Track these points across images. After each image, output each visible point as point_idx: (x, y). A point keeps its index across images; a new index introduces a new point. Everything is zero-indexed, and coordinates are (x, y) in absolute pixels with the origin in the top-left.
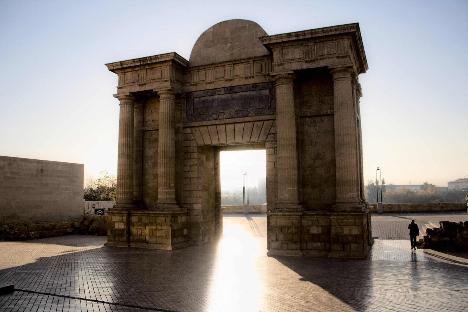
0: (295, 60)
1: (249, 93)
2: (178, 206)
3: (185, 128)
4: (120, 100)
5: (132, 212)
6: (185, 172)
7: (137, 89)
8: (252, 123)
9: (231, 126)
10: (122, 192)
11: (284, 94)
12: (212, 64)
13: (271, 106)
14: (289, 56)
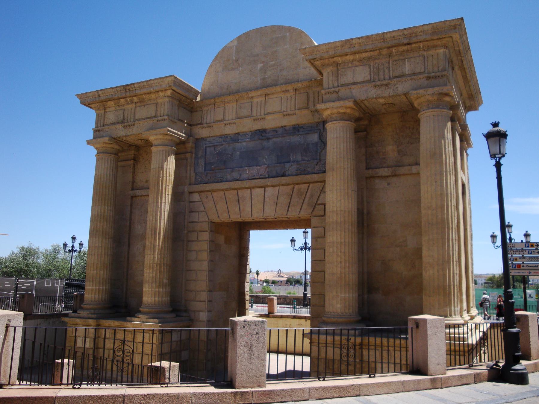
2: (173, 315)
3: (191, 193)
4: (96, 148)
6: (188, 261)
7: (120, 131)
8: (290, 187)
9: (260, 191)
10: (92, 290)
13: (320, 160)
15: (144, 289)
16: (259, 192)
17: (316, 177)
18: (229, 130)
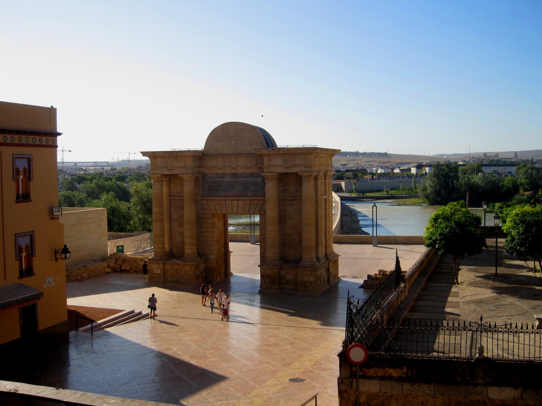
0: (277, 166)
1: (248, 179)
5: (167, 261)
7: (166, 172)
11: (271, 188)
12: (222, 155)
15: (185, 247)
16: (235, 203)
17: (261, 198)
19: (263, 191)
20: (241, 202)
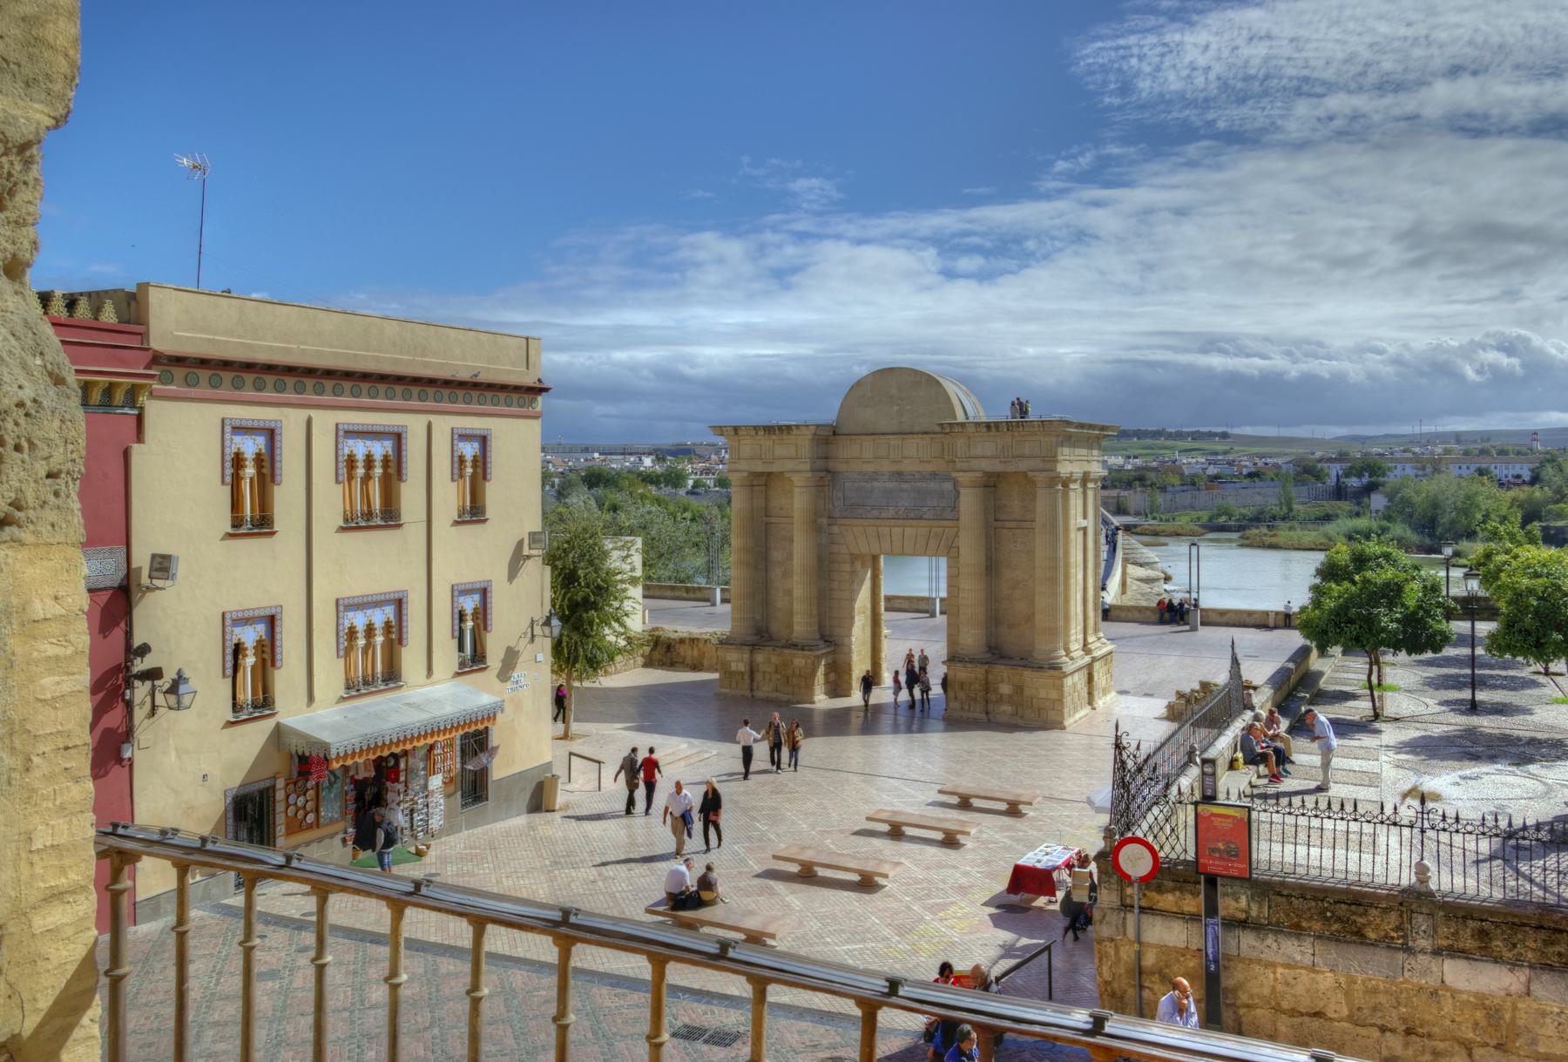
7: (759, 467)
9: (899, 530)
11: (969, 502)
14: (978, 451)
16: (897, 531)
17: (950, 523)
18: (868, 468)
19: (955, 508)
20: (909, 531)
